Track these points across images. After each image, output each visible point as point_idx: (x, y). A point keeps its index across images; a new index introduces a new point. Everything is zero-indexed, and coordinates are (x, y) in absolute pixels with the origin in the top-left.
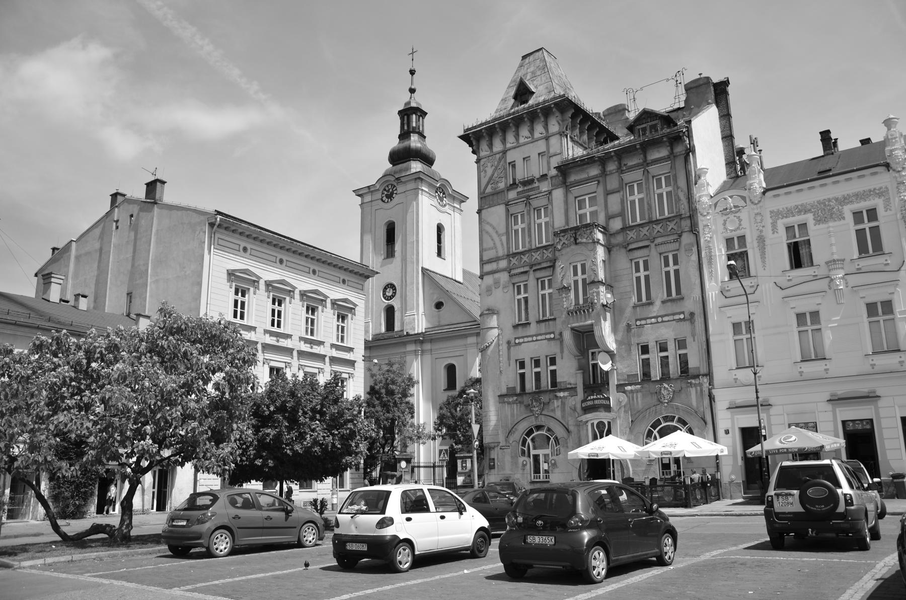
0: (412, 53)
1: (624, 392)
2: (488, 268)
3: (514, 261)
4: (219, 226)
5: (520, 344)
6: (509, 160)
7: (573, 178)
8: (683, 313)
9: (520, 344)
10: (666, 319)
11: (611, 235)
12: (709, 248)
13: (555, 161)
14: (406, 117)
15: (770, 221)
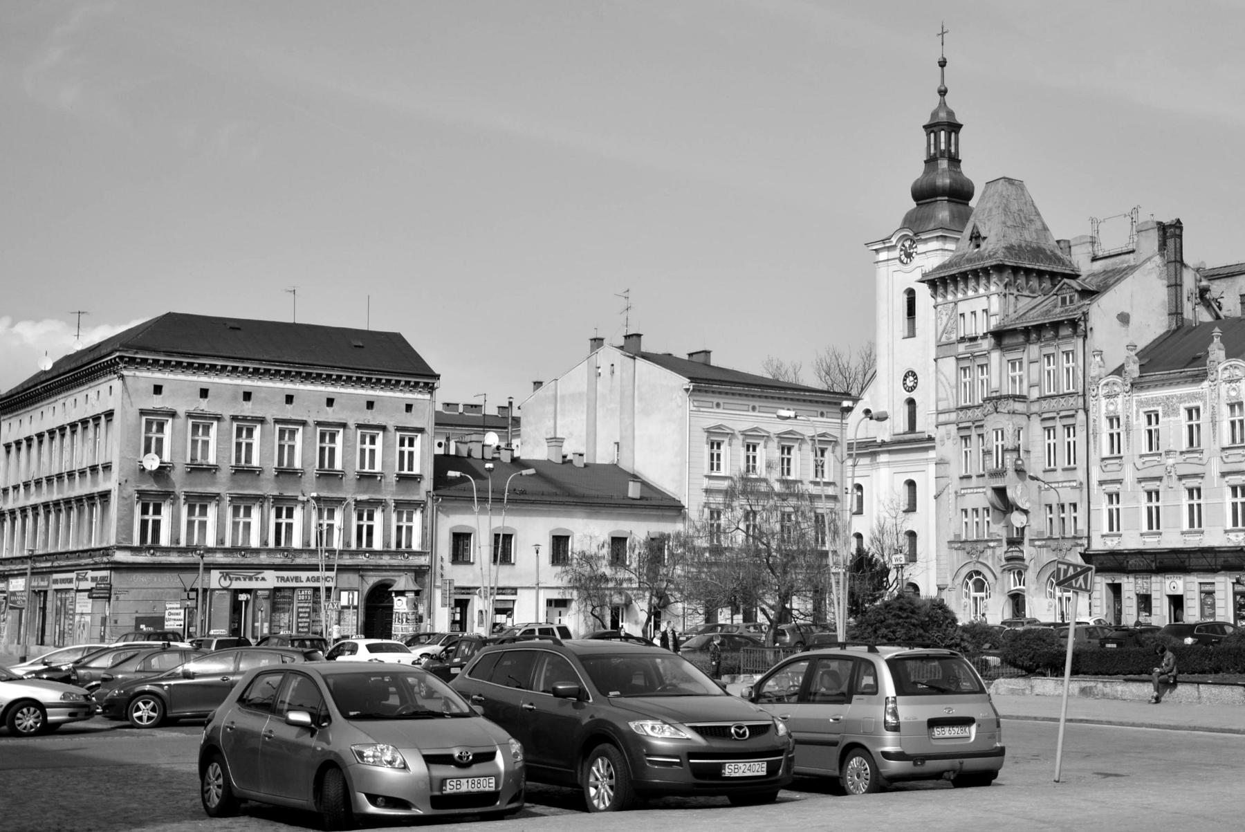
0: (943, 33)
1: (1034, 546)
2: (943, 418)
3: (961, 414)
4: (694, 390)
5: (964, 495)
6: (960, 312)
7: (1006, 341)
8: (1075, 481)
9: (964, 495)
10: (1065, 484)
11: (1031, 402)
12: (1095, 425)
13: (994, 323)
14: (932, 135)
15: (1135, 408)
